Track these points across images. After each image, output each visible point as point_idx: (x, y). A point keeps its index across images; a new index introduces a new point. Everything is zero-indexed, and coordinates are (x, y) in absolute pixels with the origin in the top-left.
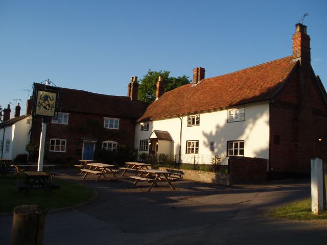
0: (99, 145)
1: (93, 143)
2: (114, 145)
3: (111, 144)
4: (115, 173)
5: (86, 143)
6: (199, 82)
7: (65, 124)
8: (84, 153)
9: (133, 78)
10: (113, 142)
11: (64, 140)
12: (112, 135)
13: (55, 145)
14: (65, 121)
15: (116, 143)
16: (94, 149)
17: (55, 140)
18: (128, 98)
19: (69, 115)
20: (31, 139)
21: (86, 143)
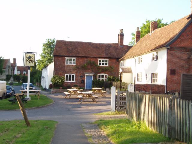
0: (95, 77)
1: (92, 76)
2: (106, 76)
3: (104, 76)
4: (103, 93)
5: (87, 76)
6: (153, 32)
7: (73, 64)
8: (86, 83)
9: (120, 30)
10: (105, 75)
11: (73, 74)
12: (104, 70)
13: (68, 78)
14: (74, 63)
15: (107, 75)
16: (93, 79)
17: (68, 75)
18: (117, 44)
19: (76, 59)
20: (54, 75)
21: (87, 76)
